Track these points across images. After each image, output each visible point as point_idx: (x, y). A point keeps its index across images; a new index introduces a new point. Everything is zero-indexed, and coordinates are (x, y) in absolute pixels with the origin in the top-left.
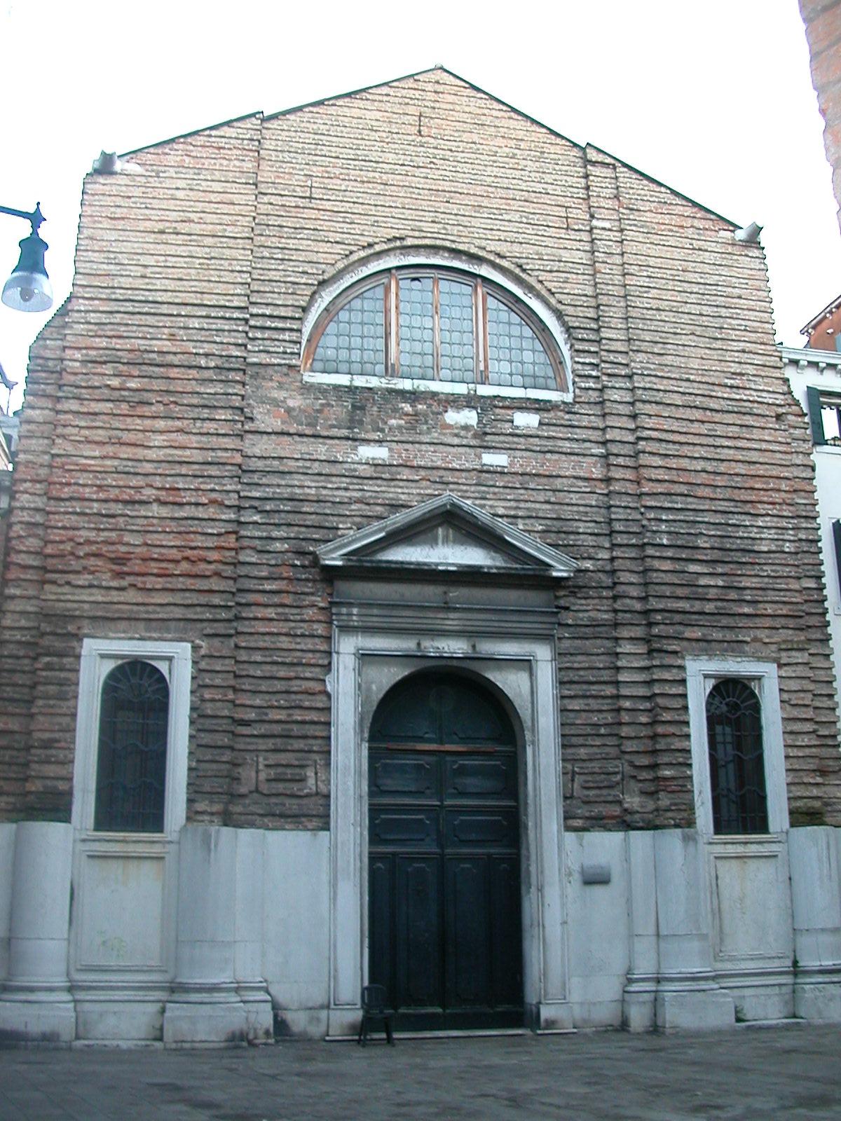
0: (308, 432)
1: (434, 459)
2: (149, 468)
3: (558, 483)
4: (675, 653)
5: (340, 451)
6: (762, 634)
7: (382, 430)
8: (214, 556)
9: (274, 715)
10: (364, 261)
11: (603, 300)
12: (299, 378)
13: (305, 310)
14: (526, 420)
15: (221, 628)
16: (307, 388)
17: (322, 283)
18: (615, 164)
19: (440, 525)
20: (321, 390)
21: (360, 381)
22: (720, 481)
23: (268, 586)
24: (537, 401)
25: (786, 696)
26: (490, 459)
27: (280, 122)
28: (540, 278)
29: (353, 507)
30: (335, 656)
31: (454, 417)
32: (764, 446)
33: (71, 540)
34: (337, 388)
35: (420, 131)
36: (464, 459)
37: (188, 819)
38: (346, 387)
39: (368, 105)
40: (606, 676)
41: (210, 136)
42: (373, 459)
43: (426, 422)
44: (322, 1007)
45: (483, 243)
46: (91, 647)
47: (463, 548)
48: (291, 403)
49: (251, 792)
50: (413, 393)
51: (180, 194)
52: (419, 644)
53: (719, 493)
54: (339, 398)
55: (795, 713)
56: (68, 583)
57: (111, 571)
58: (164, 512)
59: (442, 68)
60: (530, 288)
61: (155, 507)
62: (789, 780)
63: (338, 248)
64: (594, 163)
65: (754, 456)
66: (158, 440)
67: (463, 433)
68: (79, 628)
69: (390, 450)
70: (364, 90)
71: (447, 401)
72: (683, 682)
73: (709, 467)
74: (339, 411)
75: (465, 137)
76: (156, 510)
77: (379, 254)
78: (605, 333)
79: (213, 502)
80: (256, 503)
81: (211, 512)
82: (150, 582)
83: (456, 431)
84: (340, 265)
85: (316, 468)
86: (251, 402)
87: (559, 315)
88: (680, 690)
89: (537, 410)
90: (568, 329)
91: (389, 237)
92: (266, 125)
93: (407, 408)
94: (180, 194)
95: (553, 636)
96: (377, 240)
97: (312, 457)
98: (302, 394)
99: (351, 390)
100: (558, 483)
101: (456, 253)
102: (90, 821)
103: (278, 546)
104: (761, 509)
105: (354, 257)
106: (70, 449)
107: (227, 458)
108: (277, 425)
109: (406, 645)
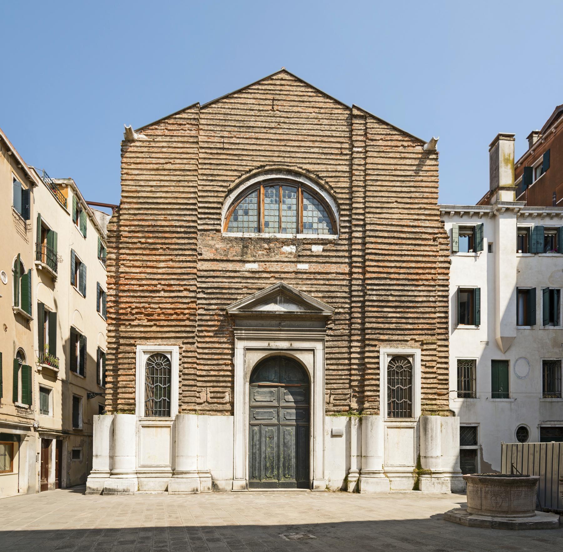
0: (225, 258)
1: (277, 268)
2: (159, 277)
3: (330, 276)
4: (375, 346)
5: (238, 266)
6: (416, 337)
7: (255, 256)
8: (186, 311)
9: (212, 373)
10: (248, 179)
11: (355, 189)
12: (220, 235)
13: (222, 204)
14: (317, 249)
15: (191, 340)
16: (223, 239)
17: (230, 191)
18: (366, 116)
19: (278, 295)
20: (230, 240)
21: (247, 235)
22: (402, 271)
23: (210, 323)
24: (322, 239)
25: (424, 363)
27: (209, 109)
28: (327, 181)
29: (243, 290)
30: (236, 350)
31: (287, 249)
32: (425, 253)
33: (130, 307)
34: (236, 238)
35: (273, 108)
36: (291, 268)
37: (180, 412)
38: (240, 238)
39: (249, 96)
40: (346, 356)
41: (176, 118)
42: (252, 269)
43: (274, 251)
45: (301, 165)
46: (139, 349)
47: (288, 305)
48: (217, 246)
49: (204, 402)
50: (269, 239)
51: (164, 150)
53: (401, 276)
54: (237, 243)
55: (428, 370)
56: (130, 324)
57: (146, 319)
58: (166, 294)
59: (284, 71)
60: (322, 187)
61: (162, 292)
62: (422, 397)
63: (236, 173)
64: (356, 117)
65: (420, 259)
66: (162, 265)
67: (289, 256)
68: (135, 342)
69: (259, 265)
70: (247, 88)
71: (283, 243)
72: (378, 357)
73: (398, 264)
74: (238, 248)
75: (295, 109)
77: (255, 175)
78: (354, 205)
79: (186, 290)
81: (185, 293)
82: (162, 323)
83: (287, 255)
84: (237, 181)
85: (228, 274)
86: (201, 246)
87: (335, 199)
88: (376, 360)
89: (322, 244)
90: (338, 205)
91: (258, 165)
92: (202, 111)
93: (266, 246)
94: (164, 150)
95: (324, 340)
96: (253, 168)
97: (226, 269)
98: (222, 242)
99: (242, 239)
100: (330, 276)
101: (289, 172)
102: (143, 413)
103: (213, 307)
104: (420, 283)
105: (244, 177)
106: (127, 270)
107: (191, 271)
108: (212, 256)
109: (264, 344)
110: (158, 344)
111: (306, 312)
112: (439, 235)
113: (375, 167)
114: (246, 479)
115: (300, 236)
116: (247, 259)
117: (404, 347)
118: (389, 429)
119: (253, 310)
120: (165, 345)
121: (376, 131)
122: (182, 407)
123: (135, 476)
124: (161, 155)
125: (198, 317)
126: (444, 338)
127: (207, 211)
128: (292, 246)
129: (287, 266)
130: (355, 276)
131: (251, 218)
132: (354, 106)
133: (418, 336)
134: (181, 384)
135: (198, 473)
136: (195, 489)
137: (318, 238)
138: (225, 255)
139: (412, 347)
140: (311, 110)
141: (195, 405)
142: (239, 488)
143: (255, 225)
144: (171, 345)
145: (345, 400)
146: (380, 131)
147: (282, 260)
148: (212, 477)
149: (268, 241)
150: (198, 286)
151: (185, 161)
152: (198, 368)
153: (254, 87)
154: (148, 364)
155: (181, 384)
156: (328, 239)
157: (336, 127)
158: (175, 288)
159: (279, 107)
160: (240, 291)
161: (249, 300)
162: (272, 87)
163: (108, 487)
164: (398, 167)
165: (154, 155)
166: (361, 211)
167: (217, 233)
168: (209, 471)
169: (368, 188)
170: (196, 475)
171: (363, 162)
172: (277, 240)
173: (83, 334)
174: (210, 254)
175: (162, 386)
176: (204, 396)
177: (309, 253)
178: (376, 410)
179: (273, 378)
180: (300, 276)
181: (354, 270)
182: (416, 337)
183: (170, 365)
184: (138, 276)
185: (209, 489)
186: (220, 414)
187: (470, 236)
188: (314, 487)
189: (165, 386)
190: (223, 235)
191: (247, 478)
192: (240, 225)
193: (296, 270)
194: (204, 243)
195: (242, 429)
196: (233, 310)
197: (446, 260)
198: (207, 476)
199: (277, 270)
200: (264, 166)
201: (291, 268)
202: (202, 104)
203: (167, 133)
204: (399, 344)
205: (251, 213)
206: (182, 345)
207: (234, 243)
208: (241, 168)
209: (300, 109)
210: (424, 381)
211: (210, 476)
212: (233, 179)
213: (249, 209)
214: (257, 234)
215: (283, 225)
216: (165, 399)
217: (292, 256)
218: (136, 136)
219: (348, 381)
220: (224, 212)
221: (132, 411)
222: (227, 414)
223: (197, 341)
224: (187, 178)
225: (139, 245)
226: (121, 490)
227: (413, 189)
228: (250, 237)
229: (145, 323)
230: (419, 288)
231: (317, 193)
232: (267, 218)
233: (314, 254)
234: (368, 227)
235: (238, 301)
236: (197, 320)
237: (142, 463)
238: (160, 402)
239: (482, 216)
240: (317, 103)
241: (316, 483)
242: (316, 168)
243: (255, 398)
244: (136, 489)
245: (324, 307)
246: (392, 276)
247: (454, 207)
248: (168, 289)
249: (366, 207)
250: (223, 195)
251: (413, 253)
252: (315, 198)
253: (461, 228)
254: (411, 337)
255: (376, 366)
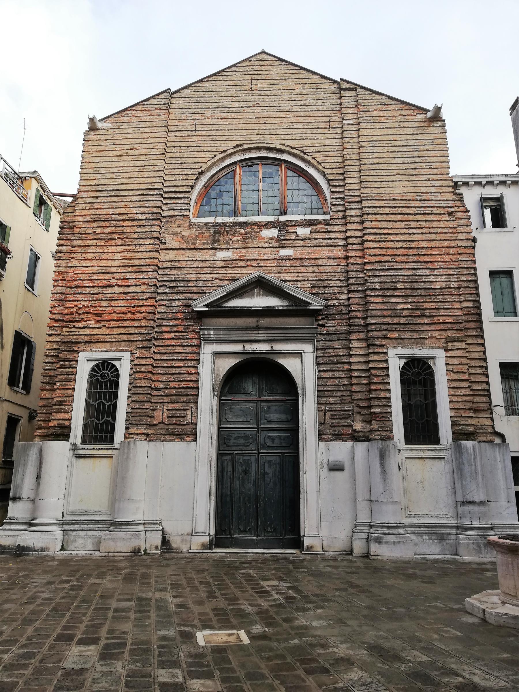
0: (192, 247)
1: (255, 255)
2: (113, 270)
3: (320, 262)
4: (383, 346)
5: (207, 255)
6: (436, 334)
7: (229, 243)
8: (143, 309)
9: (172, 385)
10: (223, 159)
11: (347, 163)
12: (189, 221)
13: (192, 187)
14: (303, 231)
15: (145, 344)
16: (191, 226)
17: (201, 173)
18: (355, 88)
19: (256, 287)
20: (199, 226)
21: (219, 220)
22: (411, 252)
23: (171, 323)
24: (310, 220)
25: (450, 367)
26: (283, 253)
27: (181, 94)
28: (313, 156)
29: (214, 282)
30: (201, 355)
31: (267, 233)
32: (439, 230)
33: (76, 306)
34: (206, 224)
35: (251, 88)
36: (271, 254)
37: (125, 437)
38: (211, 223)
39: (225, 78)
40: (344, 359)
41: (144, 105)
42: (224, 257)
43: (251, 237)
44: (188, 534)
45: (283, 142)
46: (82, 356)
47: (268, 298)
48: (184, 233)
49: (159, 423)
50: (245, 223)
51: (130, 136)
52: (244, 347)
53: (411, 259)
54: (208, 229)
55: (456, 377)
56: (74, 327)
57: (95, 320)
58: (120, 290)
59: (263, 52)
60: (308, 163)
61: (116, 287)
62: (452, 414)
63: (208, 154)
64: (345, 89)
65: (433, 237)
66: (118, 256)
67: (270, 241)
68: (79, 348)
69: (233, 252)
70: (223, 71)
71: (262, 226)
72: (386, 361)
73: (405, 245)
74: (209, 234)
75: (276, 87)
76: (116, 289)
77: (231, 155)
78: (347, 181)
79: (144, 284)
80: (166, 284)
81: (143, 288)
82: (113, 324)
83: (266, 240)
84: (210, 163)
85: (196, 264)
86: (165, 235)
87: (324, 175)
88: (385, 366)
89: (310, 225)
90: (329, 181)
91: (234, 145)
92: (173, 96)
93: (242, 231)
94: (130, 136)
95: (314, 340)
96: (228, 148)
97: (194, 259)
98: (190, 229)
99: (214, 225)
100: (320, 262)
101: (270, 149)
102: (79, 441)
103: (177, 303)
104: (436, 265)
105: (217, 158)
106: (77, 263)
107: (150, 262)
108: (177, 245)
109: (238, 347)
110: (106, 349)
111: (289, 306)
112: (456, 209)
113: (370, 138)
114: (209, 534)
115: (283, 218)
116: (219, 247)
117: (421, 348)
118: (408, 460)
119: (224, 305)
120: (113, 351)
121: (369, 103)
122: (130, 430)
123: (60, 528)
124: (125, 142)
125: (157, 316)
126: (476, 334)
127: (173, 195)
128: (272, 229)
129: (266, 253)
130: (351, 261)
131: (226, 201)
132: (341, 79)
133: (439, 332)
134: (131, 399)
135: (144, 524)
136: (137, 548)
137: (305, 220)
138: (192, 244)
139: (432, 348)
140: (294, 87)
141: (146, 428)
142: (200, 548)
143: (231, 208)
144: (121, 351)
145: (346, 418)
146: (373, 102)
147: (261, 245)
148: (163, 530)
149: (244, 225)
150: (159, 279)
151: (151, 146)
152: (154, 379)
153: (231, 70)
154: (91, 376)
155: (131, 399)
156: (316, 220)
157: (322, 101)
158: (132, 282)
159: (259, 86)
160: (209, 284)
161: (221, 293)
162: (250, 68)
163: (21, 544)
164: (398, 137)
165: (118, 142)
166: (356, 186)
167: (184, 219)
168: (158, 522)
169: (364, 161)
170: (141, 528)
171: (355, 134)
172: (255, 223)
173: (32, 340)
174: (175, 243)
175: (106, 403)
176: (158, 416)
177: (293, 236)
178: (388, 433)
179: (250, 390)
180: (283, 263)
181: (352, 254)
182: (436, 334)
183: (118, 376)
184: (89, 270)
185: (157, 548)
186: (179, 440)
187: (492, 208)
188: (305, 548)
189: (109, 403)
190: (192, 221)
191: (212, 532)
192: (213, 209)
193: (278, 257)
194: (168, 230)
195: (206, 461)
196: (200, 306)
197: (467, 237)
198: (156, 529)
199: (255, 258)
200: (241, 146)
201: (271, 254)
202: (173, 90)
203: (134, 119)
204: (413, 343)
205: (225, 195)
206: (134, 351)
207: (204, 230)
208: (214, 149)
209: (280, 87)
210: (453, 392)
211: (161, 528)
212: (204, 160)
213: (223, 192)
214: (231, 218)
215: (264, 207)
216: (109, 420)
217: (273, 241)
218: (100, 125)
219: (348, 393)
220: (194, 196)
221: (65, 437)
222: (187, 439)
223: (154, 345)
224: (152, 162)
225: (94, 236)
226: (37, 549)
227: (417, 160)
228: (224, 221)
229: (93, 324)
230: (436, 272)
231: (303, 170)
232: (245, 200)
233: (299, 237)
234: (365, 204)
235: (207, 294)
236: (156, 319)
237: (72, 509)
238: (102, 424)
239: (509, 185)
240: (301, 80)
241: (307, 542)
242: (301, 143)
243: (226, 417)
244: (59, 547)
245: (312, 299)
246: (399, 259)
247: (473, 176)
248: (124, 283)
249: (361, 182)
250: (194, 177)
251: (423, 231)
252: (301, 176)
253: (484, 200)
254: (430, 333)
255: (385, 372)
